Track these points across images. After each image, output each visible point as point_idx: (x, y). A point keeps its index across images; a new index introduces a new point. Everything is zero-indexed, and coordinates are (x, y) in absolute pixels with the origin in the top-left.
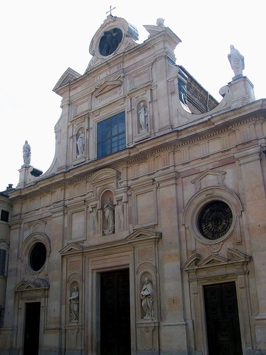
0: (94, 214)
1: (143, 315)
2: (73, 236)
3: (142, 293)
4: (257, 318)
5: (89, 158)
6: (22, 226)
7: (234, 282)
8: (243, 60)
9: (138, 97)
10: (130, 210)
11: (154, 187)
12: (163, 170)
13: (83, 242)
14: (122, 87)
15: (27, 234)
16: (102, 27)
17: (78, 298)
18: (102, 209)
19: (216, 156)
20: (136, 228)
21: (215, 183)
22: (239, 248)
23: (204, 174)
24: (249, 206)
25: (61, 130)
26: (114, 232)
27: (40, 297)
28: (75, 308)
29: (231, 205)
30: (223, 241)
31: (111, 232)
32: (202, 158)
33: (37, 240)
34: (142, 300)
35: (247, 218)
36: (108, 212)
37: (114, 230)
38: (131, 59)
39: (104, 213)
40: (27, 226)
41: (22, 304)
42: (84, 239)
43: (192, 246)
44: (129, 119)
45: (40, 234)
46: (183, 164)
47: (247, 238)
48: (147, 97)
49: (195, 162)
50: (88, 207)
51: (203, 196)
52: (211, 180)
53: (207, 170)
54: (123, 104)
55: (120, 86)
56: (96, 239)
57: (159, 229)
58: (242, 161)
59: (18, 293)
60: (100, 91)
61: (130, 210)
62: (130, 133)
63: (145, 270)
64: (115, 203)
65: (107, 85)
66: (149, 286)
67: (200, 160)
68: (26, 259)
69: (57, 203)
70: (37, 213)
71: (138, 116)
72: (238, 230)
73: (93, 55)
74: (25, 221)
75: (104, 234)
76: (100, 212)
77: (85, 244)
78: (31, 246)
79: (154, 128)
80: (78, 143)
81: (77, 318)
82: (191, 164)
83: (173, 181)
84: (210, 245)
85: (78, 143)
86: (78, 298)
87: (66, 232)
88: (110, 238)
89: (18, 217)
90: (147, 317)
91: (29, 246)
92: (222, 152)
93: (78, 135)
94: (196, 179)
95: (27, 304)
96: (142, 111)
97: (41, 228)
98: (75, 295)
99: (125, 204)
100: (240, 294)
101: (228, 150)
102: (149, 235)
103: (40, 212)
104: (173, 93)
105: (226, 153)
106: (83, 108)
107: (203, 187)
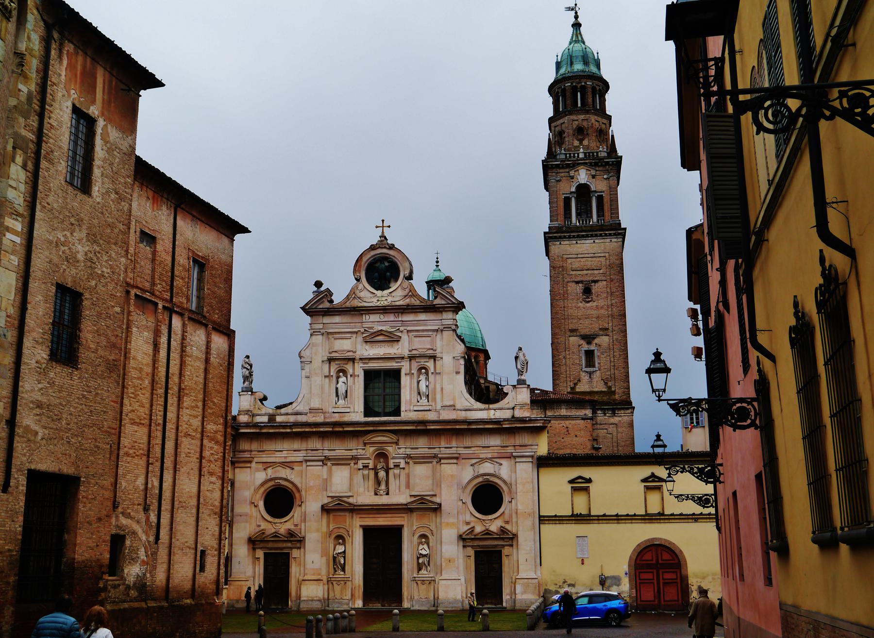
0: (366, 472)
1: (420, 569)
2: (333, 489)
3: (420, 552)
4: (517, 577)
5: (354, 409)
6: (253, 465)
7: (501, 551)
8: (527, 363)
9: (420, 362)
10: (408, 476)
11: (435, 461)
12: (446, 448)
13: (348, 497)
14: (400, 343)
15: (261, 476)
16: (373, 248)
17: (344, 552)
18: (375, 469)
19: (495, 448)
20: (413, 493)
21: (492, 471)
22: (508, 527)
23: (483, 460)
24: (520, 496)
25: (311, 362)
26: (388, 494)
27: (291, 548)
28: (342, 562)
29: (504, 492)
30: (495, 519)
31: (385, 493)
32: (483, 447)
33: (279, 485)
34: (418, 558)
35: (517, 504)
36: (382, 474)
37: (388, 491)
38: (412, 312)
39: (376, 474)
40: (260, 466)
41: (260, 554)
42: (351, 494)
43: (468, 518)
44: (405, 381)
45: (286, 480)
46: (465, 448)
47: (514, 520)
48: (430, 364)
49: (476, 448)
50: (356, 463)
51: (480, 479)
52: (487, 468)
53: (487, 458)
54: (400, 362)
55: (399, 341)
56: (365, 496)
57: (437, 500)
58: (518, 460)
59: (253, 542)
60: (371, 338)
61: (408, 476)
62: (408, 398)
63: (426, 533)
64: (391, 465)
65: (382, 334)
66: (425, 546)
67: (481, 448)
68: (261, 504)
69: (312, 450)
70: (278, 454)
71: (418, 382)
72: (507, 512)
73: (358, 280)
74: (256, 460)
75: (376, 494)
76: (372, 473)
77: (351, 500)
78: (268, 491)
79: (435, 400)
80: (339, 386)
81: (343, 570)
82: (473, 449)
83: (455, 461)
84: (483, 520)
85: (339, 386)
86: (344, 552)
87: (326, 484)
88: (384, 500)
89: (247, 455)
90: (423, 572)
91: (265, 490)
92: (502, 447)
93: (338, 377)
94: (475, 463)
95: (265, 553)
96: (423, 377)
97: (284, 473)
98: (340, 549)
99: (402, 470)
100: (505, 561)
101: (507, 446)
102: (430, 504)
103: (284, 454)
104: (458, 373)
105: (505, 448)
106: (344, 345)
107: (482, 472)
